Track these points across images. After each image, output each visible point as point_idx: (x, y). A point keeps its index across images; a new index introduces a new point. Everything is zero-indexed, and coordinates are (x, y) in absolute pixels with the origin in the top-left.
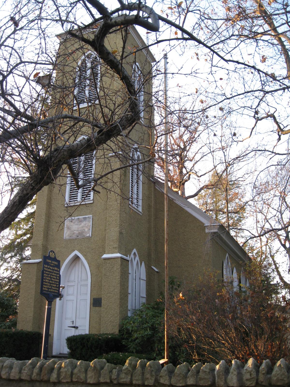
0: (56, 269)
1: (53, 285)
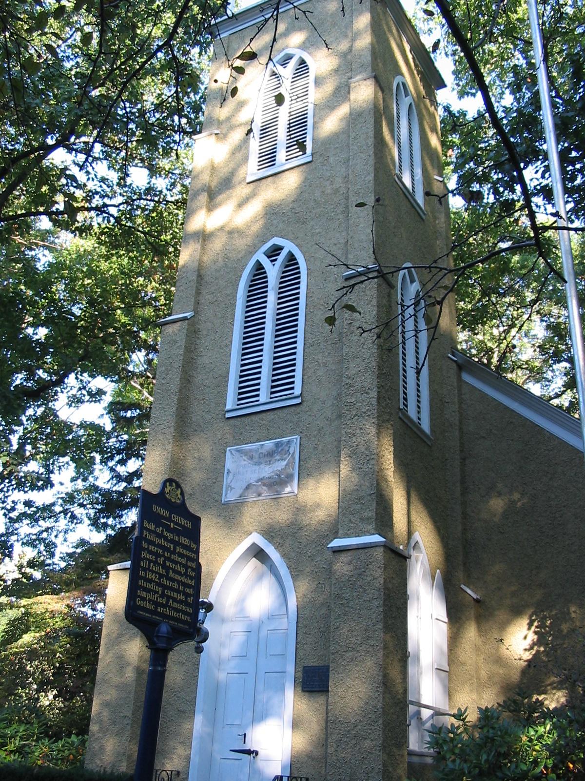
0: (185, 541)
1: (175, 595)
